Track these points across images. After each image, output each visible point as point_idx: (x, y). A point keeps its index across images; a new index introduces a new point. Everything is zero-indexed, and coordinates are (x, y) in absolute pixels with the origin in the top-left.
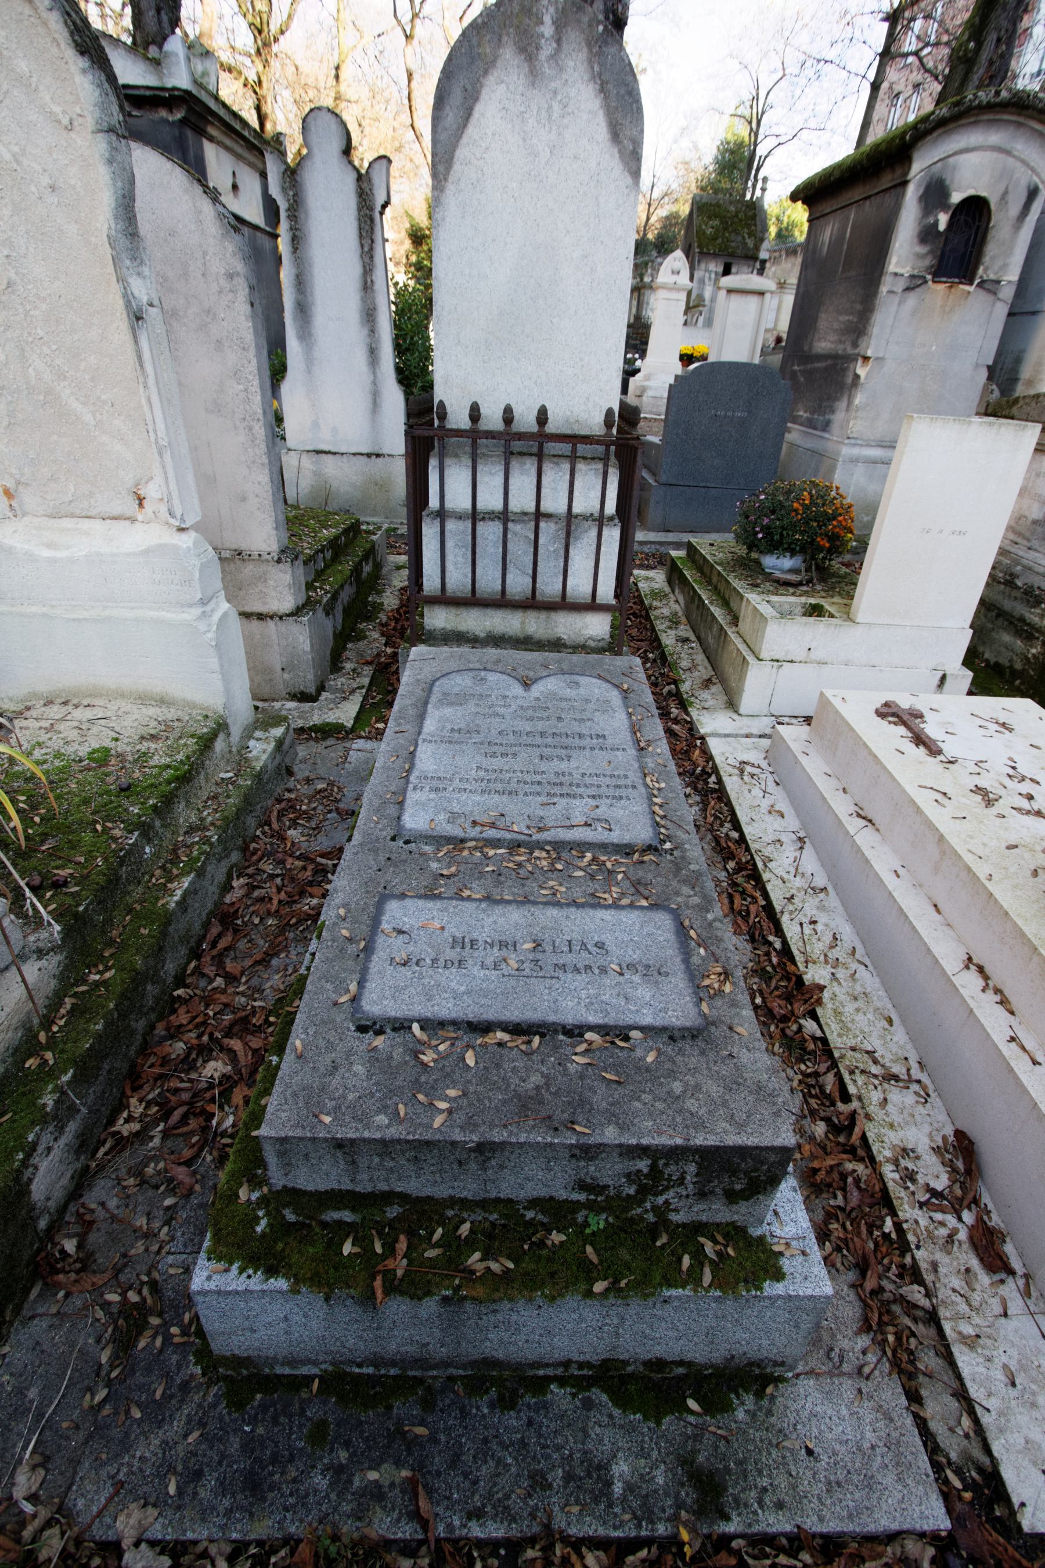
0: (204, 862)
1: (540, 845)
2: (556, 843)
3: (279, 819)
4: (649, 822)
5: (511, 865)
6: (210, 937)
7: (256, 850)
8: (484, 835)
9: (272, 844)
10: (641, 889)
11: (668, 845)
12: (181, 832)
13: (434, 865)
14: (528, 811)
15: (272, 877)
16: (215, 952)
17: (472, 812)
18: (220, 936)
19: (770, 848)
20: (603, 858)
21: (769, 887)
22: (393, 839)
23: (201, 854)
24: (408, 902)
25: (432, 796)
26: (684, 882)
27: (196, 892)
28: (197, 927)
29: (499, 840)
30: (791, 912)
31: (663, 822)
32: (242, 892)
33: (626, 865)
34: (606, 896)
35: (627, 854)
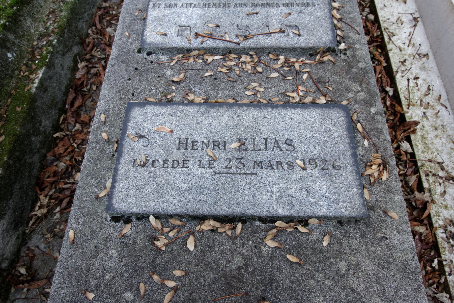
0: (50, 59)
1: (245, 51)
2: (258, 49)
3: (101, 22)
4: (329, 26)
5: (224, 70)
6: (69, 101)
7: (89, 43)
8: (204, 45)
9: (98, 39)
10: (321, 87)
11: (342, 46)
12: (35, 38)
13: (169, 73)
14: (237, 21)
15: (100, 59)
16: (72, 110)
17: (195, 24)
18: (75, 99)
19: (394, 26)
20: (293, 60)
21: (390, 54)
22: (139, 52)
23: (47, 53)
24: (148, 109)
25: (167, 11)
26: (353, 79)
27: (50, 78)
28: (59, 96)
29: (215, 49)
30: (403, 72)
31: (339, 25)
32: (84, 71)
33: (310, 65)
34: (294, 95)
35: (311, 55)
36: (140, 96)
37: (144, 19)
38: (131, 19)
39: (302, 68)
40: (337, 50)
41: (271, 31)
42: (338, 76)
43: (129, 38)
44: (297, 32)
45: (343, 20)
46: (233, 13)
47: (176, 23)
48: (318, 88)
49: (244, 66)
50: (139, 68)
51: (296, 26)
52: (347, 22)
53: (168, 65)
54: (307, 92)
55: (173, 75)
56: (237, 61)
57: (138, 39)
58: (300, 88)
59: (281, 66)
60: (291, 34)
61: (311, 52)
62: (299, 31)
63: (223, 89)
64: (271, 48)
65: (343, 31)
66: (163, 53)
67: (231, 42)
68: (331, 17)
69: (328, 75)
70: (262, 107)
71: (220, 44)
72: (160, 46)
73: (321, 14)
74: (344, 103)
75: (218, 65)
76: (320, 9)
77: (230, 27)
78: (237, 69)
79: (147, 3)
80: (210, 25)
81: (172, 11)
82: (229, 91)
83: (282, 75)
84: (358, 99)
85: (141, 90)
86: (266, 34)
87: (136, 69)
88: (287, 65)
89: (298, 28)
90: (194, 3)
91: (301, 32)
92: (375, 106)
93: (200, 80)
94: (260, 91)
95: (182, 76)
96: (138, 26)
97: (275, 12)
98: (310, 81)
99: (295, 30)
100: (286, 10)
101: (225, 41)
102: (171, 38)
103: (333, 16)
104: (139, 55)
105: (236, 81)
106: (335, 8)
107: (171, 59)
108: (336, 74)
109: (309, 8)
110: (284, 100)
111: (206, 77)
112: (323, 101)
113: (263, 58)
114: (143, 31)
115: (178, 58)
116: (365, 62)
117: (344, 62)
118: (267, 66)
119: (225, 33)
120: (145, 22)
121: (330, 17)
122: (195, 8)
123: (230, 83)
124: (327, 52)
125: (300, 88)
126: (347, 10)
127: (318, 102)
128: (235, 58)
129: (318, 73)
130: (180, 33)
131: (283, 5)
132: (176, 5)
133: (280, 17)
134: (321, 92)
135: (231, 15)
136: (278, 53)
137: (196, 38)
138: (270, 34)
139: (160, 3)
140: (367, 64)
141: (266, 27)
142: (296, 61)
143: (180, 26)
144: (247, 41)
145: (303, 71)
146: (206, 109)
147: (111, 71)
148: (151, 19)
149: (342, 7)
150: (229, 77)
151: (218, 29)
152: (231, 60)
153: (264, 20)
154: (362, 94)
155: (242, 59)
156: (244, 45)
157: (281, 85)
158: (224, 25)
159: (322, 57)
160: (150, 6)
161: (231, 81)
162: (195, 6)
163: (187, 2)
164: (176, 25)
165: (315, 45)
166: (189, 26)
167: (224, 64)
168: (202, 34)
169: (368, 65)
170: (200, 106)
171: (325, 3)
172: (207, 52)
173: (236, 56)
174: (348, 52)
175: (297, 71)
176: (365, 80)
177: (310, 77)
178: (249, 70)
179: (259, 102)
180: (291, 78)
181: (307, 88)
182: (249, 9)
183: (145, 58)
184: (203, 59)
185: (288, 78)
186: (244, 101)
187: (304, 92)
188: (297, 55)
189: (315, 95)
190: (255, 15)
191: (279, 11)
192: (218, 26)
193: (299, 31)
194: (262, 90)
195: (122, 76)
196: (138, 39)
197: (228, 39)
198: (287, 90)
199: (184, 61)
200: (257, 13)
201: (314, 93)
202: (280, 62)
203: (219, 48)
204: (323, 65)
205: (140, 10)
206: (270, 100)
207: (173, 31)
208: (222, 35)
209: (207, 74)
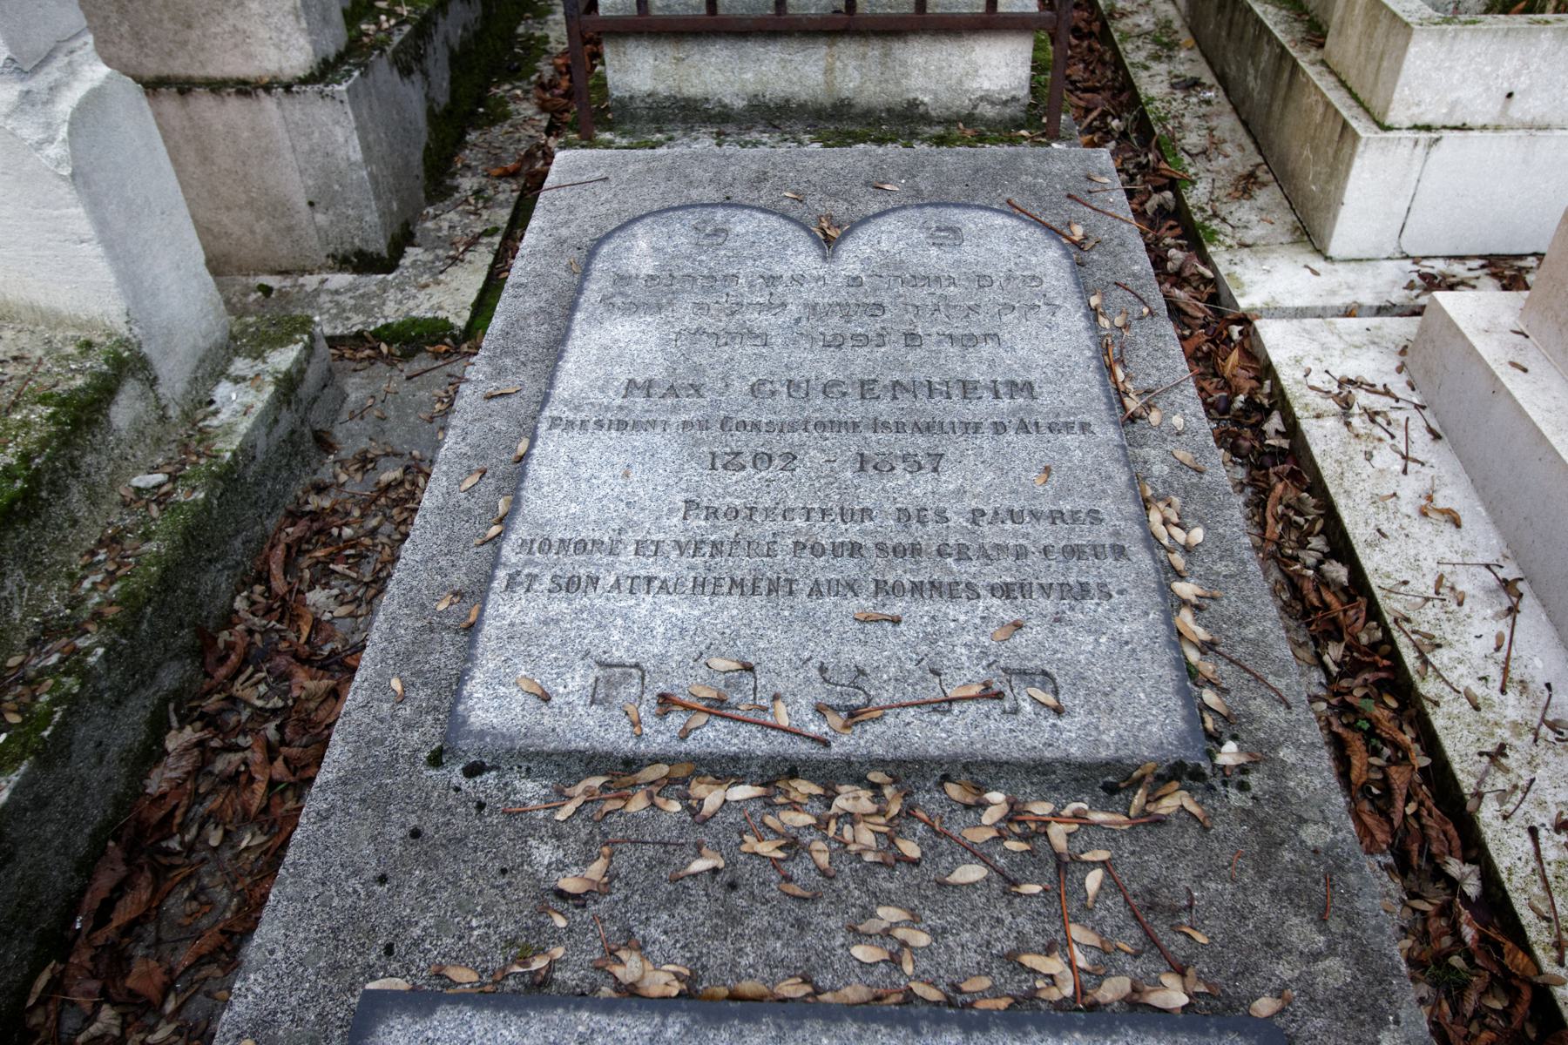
0: (63, 724)
1: (853, 771)
2: (900, 763)
3: (289, 566)
4: (1169, 674)
5: (767, 848)
6: (91, 901)
7: (230, 646)
8: (690, 745)
9: (266, 632)
10: (1161, 929)
11: (1229, 754)
12: (20, 641)
13: (544, 853)
14: (822, 650)
15: (262, 715)
16: (100, 938)
17: (662, 658)
18: (120, 889)
19: (1431, 611)
20: (1042, 809)
21: (1438, 722)
22: (436, 760)
23: (54, 702)
24: (446, 1023)
25: (559, 606)
26: (1288, 895)
27: (41, 803)
28: (59, 876)
29: (735, 759)
30: (1503, 796)
31: (1207, 667)
32: (186, 764)
33: (1111, 836)
34: (1054, 965)
35: (1111, 789)
36: (417, 956)
37: (472, 629)
38: (418, 624)
39: (1079, 844)
40: (1208, 772)
41: (951, 693)
42: (1224, 880)
43: (402, 700)
44: (1049, 699)
45: (1221, 649)
46: (807, 616)
47: (588, 653)
48: (1147, 934)
49: (848, 832)
50: (429, 830)
51: (1045, 673)
52: (1235, 656)
53: (546, 819)
54: (1106, 953)
55: (561, 866)
56: (818, 808)
57: (435, 708)
58: (1076, 931)
59: (994, 833)
60: (1027, 707)
61: (1110, 778)
62: (1056, 693)
63: (761, 933)
64: (954, 760)
65: (1223, 692)
66: (528, 769)
67: (798, 734)
68: (1175, 639)
69: (1183, 876)
70: (925, 1027)
71: (754, 743)
72: (519, 744)
73: (1135, 626)
74: (1265, 1006)
75: (744, 825)
76: (1129, 608)
77: (792, 674)
78: (820, 845)
79: (486, 568)
80: (720, 664)
81: (577, 605)
82: (786, 945)
83: (1001, 873)
84: (1320, 988)
85: (425, 929)
86: (929, 703)
87: (416, 834)
88: (1017, 829)
89: (1053, 680)
90: (662, 575)
91: (1066, 701)
92: (1397, 1022)
93: (671, 888)
94: (912, 943)
95: (596, 870)
96: (443, 656)
97: (962, 618)
98: (1115, 902)
99: (1043, 689)
100: (1004, 611)
101: (773, 728)
102: (566, 710)
103: (1180, 634)
104: (432, 772)
105: (814, 899)
106: (1184, 603)
107: (560, 793)
108: (1213, 871)
109: (1090, 604)
110: (1011, 988)
111: (695, 875)
112: (1173, 995)
113: (921, 797)
114: (461, 678)
115: (585, 792)
116: (1325, 821)
117: (1242, 822)
118: (937, 834)
119: (776, 697)
120: (472, 644)
121: (1170, 641)
122: (664, 597)
123: (791, 905)
124: (1171, 779)
125: (1076, 931)
126: (1231, 610)
127: (1156, 999)
128: (810, 796)
129: (1143, 866)
130: (601, 694)
131: (993, 590)
132: (594, 581)
133: (982, 639)
134: (1164, 954)
135: (797, 626)
136: (982, 778)
137: (663, 715)
138: (946, 705)
139: (536, 571)
140: (1335, 831)
141: (930, 676)
142: (1053, 815)
143: (602, 665)
144: (858, 729)
145: (1085, 857)
146: (688, 1030)
147: (311, 839)
148: (494, 632)
149: (1213, 598)
150: (788, 879)
151: (748, 680)
152: (794, 806)
153: (924, 648)
154: (1333, 963)
155: (841, 803)
156: (848, 749)
157: (999, 921)
158: (771, 665)
159: (1153, 798)
160: (495, 584)
161: (795, 897)
162: (664, 587)
163: (635, 573)
164: (588, 661)
165: (1121, 753)
166: (637, 666)
167: (769, 820)
168: (687, 700)
169: (1340, 836)
170: (665, 1016)
171: (1146, 589)
172: (703, 770)
173: (816, 790)
174: (1252, 779)
175: (1058, 856)
176: (1337, 902)
177: (1113, 884)
178: (868, 849)
179: (910, 997)
180: (1036, 889)
181: (1103, 933)
182: (864, 603)
183: (457, 789)
184: (684, 798)
185: (1028, 889)
186: (848, 991)
187: (1095, 954)
188: (1056, 789)
189: (1138, 967)
190: (889, 626)
191: (979, 613)
192: (748, 668)
193: (1056, 693)
194: (922, 939)
195: (353, 863)
196: (435, 708)
197: (784, 721)
198: (1023, 946)
199: (608, 806)
200: (896, 621)
201: (1136, 956)
202: (991, 816)
203: (750, 758)
204: (1162, 832)
205: (455, 594)
206: (956, 988)
207: (575, 682)
208: (765, 702)
209: (698, 865)
